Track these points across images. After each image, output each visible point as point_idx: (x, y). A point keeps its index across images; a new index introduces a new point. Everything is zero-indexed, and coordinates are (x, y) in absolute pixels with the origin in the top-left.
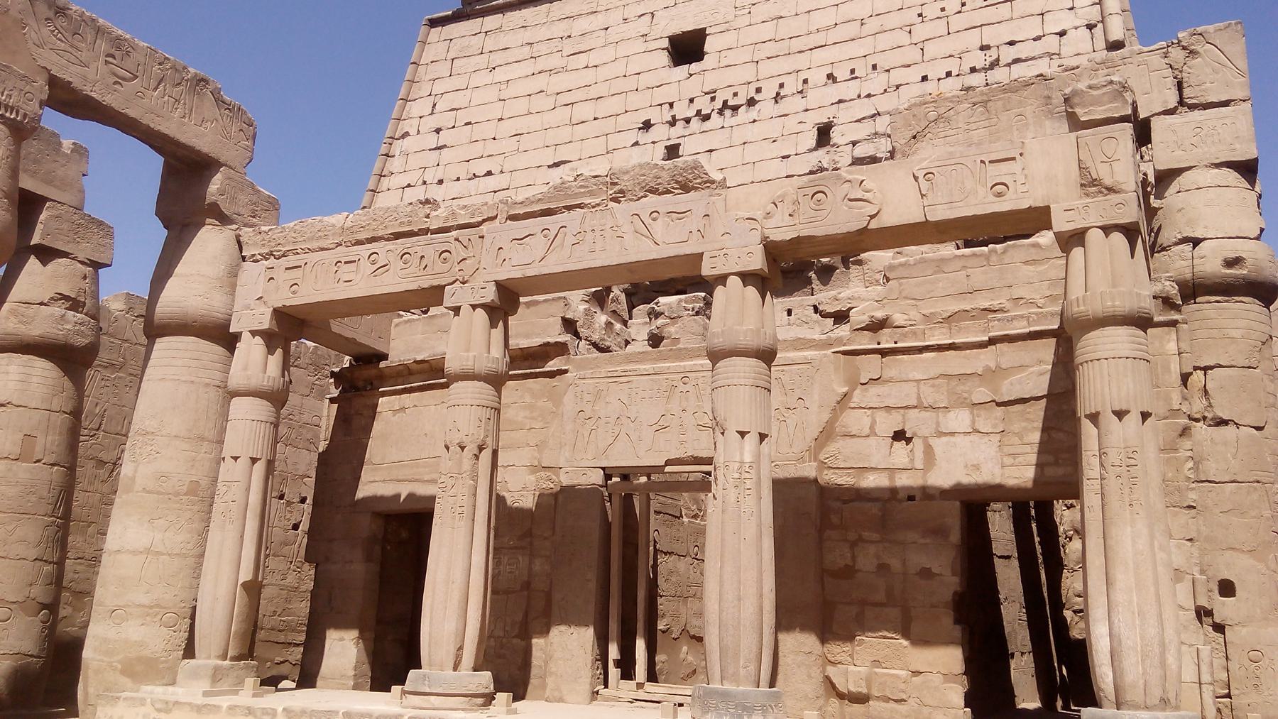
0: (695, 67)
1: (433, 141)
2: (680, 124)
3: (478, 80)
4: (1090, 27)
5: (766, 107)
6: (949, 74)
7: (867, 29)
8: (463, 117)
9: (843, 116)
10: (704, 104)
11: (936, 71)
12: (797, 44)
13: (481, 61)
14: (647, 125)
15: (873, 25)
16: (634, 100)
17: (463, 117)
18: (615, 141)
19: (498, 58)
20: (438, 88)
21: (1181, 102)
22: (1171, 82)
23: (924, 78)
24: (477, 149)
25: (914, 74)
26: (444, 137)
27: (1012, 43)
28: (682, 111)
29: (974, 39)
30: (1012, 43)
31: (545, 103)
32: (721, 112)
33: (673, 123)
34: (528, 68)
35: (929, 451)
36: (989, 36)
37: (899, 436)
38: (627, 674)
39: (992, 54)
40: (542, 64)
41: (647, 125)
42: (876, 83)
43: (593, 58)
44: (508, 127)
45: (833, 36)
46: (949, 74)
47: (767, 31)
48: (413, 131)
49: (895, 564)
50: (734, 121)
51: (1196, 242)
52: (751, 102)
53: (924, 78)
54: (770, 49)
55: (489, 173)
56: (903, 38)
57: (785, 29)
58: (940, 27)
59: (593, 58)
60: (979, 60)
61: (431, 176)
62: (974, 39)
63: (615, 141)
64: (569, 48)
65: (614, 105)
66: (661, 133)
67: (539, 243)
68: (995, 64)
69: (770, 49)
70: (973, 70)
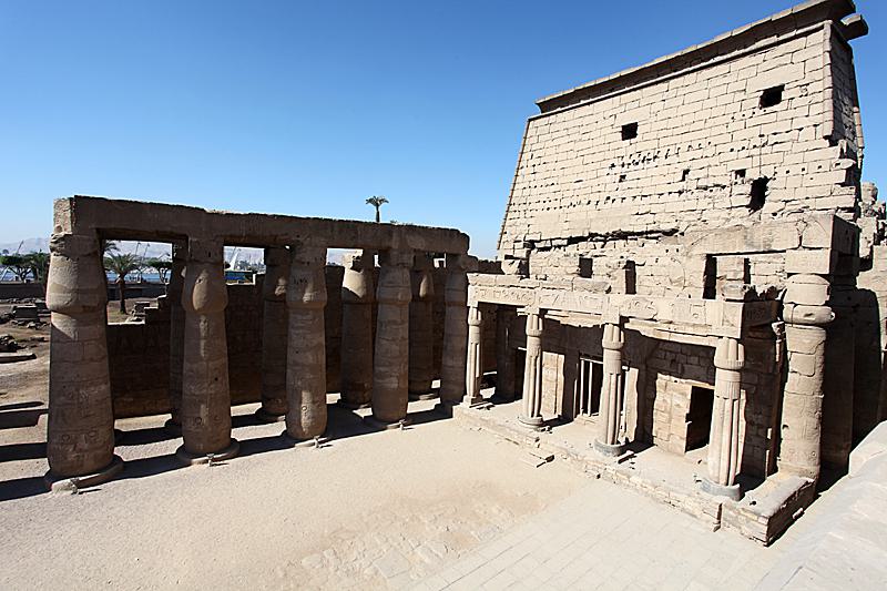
0: (633, 140)
2: (626, 166)
4: (815, 126)
5: (661, 160)
6: (743, 148)
7: (708, 125)
8: (543, 160)
9: (695, 165)
10: (635, 157)
12: (676, 131)
14: (613, 166)
16: (610, 155)
17: (543, 160)
18: (600, 172)
19: (555, 135)
21: (800, 245)
22: (797, 237)
23: (732, 150)
27: (775, 134)
28: (627, 160)
29: (757, 131)
30: (775, 134)
31: (573, 155)
32: (643, 161)
33: (623, 166)
34: (567, 139)
35: (683, 368)
36: (766, 130)
37: (673, 361)
38: (586, 411)
39: (764, 139)
40: (572, 138)
41: (613, 166)
43: (592, 135)
44: (560, 165)
45: (692, 128)
46: (743, 148)
47: (663, 124)
49: (669, 401)
50: (648, 166)
51: (796, 305)
52: (655, 157)
53: (732, 150)
54: (665, 133)
56: (724, 130)
57: (671, 123)
59: (592, 135)
61: (533, 185)
62: (757, 131)
63: (600, 172)
64: (582, 130)
65: (600, 157)
66: (618, 169)
67: (552, 299)
69: (665, 133)
70: (755, 146)
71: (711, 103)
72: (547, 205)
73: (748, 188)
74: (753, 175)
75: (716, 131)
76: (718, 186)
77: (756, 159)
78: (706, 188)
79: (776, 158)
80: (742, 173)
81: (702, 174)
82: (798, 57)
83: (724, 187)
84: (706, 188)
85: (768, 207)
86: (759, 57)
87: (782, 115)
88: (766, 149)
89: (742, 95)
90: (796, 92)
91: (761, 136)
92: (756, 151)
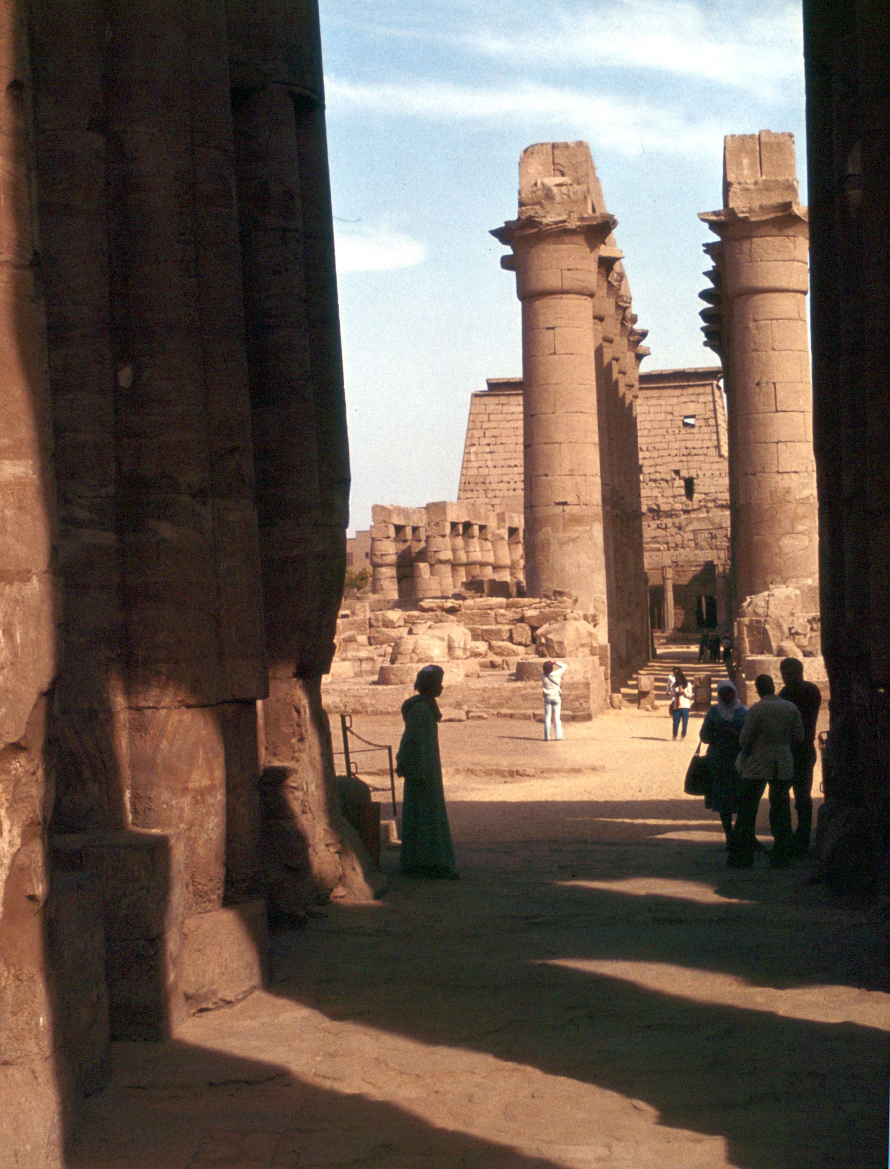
1: (488, 449)
3: (502, 425)
8: (499, 441)
11: (674, 452)
13: (500, 417)
15: (653, 433)
17: (499, 441)
19: (509, 417)
20: (485, 425)
24: (507, 455)
25: (668, 452)
26: (492, 448)
39: (688, 451)
42: (655, 454)
48: (477, 443)
55: (516, 466)
58: (672, 438)
60: (685, 452)
68: (689, 454)
71: (652, 417)
72: (512, 485)
73: (682, 483)
74: (684, 473)
75: (658, 439)
76: (662, 479)
77: (685, 463)
78: (655, 481)
79: (695, 465)
80: (677, 472)
81: (652, 470)
82: (702, 399)
83: (667, 481)
84: (655, 481)
85: (696, 497)
86: (678, 392)
87: (698, 436)
88: (689, 458)
89: (670, 417)
90: (702, 423)
91: (687, 448)
92: (684, 458)
